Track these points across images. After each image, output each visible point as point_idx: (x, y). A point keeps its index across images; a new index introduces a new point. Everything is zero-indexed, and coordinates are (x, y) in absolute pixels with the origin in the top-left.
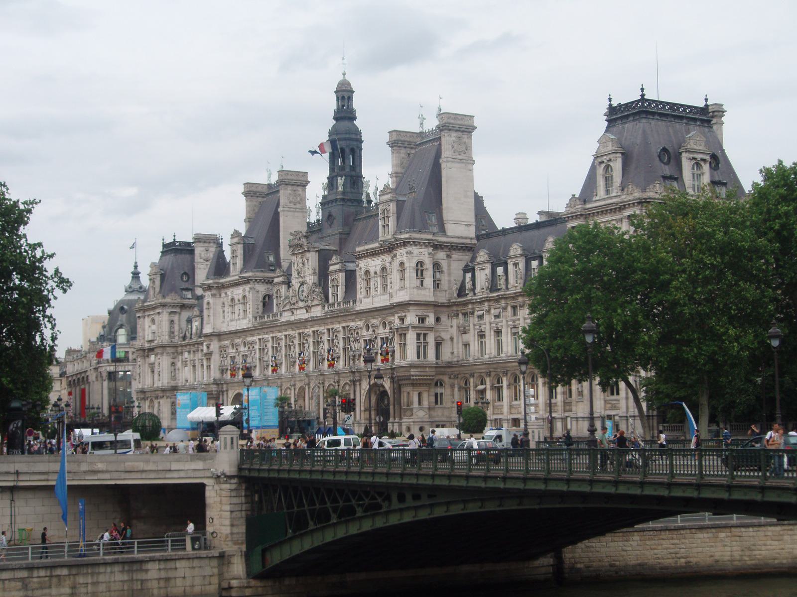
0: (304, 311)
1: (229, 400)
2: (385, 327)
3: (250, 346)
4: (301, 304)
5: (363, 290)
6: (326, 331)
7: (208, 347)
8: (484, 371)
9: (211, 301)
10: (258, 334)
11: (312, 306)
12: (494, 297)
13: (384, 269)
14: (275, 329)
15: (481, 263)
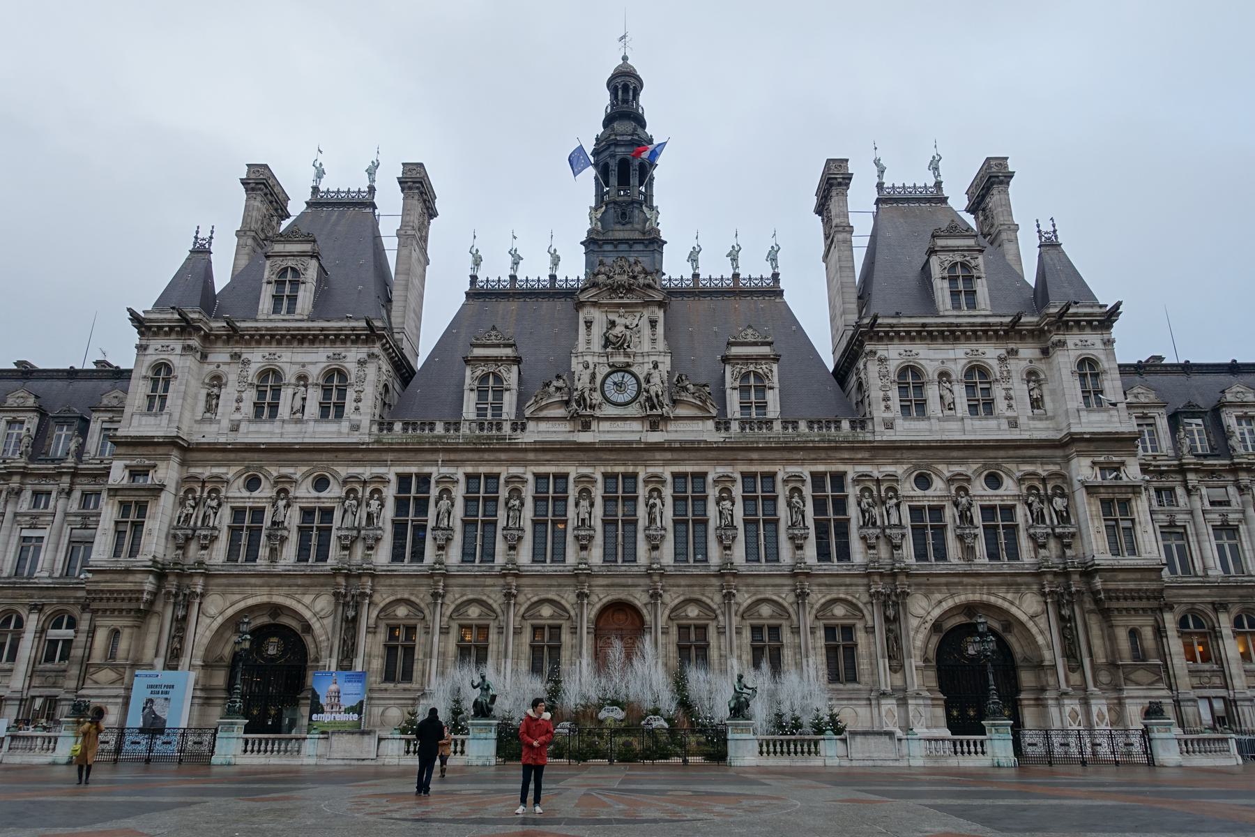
0: (636, 426)
1: (205, 621)
2: (994, 481)
3: (357, 486)
4: (610, 411)
5: (895, 403)
6: (739, 477)
7: (134, 473)
8: (1209, 599)
9: (183, 364)
10: (394, 462)
11: (677, 418)
12: (1215, 465)
13: (977, 373)
14: (486, 456)
15: (1145, 406)
